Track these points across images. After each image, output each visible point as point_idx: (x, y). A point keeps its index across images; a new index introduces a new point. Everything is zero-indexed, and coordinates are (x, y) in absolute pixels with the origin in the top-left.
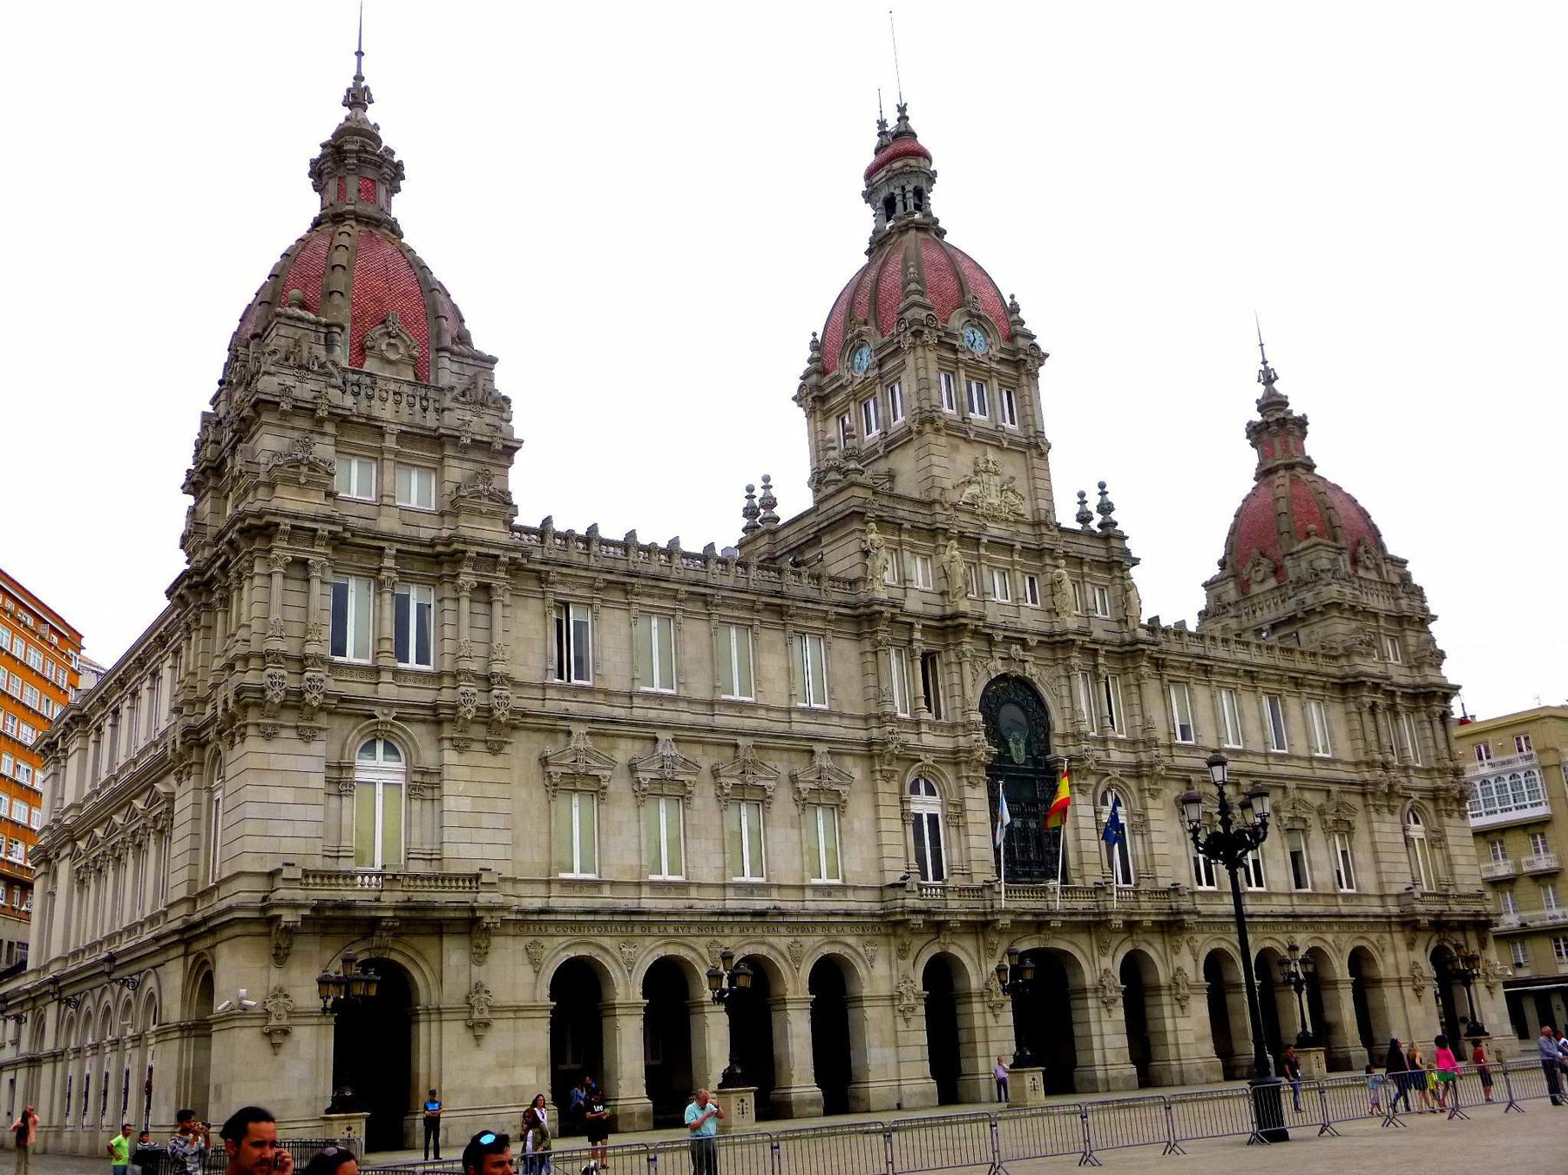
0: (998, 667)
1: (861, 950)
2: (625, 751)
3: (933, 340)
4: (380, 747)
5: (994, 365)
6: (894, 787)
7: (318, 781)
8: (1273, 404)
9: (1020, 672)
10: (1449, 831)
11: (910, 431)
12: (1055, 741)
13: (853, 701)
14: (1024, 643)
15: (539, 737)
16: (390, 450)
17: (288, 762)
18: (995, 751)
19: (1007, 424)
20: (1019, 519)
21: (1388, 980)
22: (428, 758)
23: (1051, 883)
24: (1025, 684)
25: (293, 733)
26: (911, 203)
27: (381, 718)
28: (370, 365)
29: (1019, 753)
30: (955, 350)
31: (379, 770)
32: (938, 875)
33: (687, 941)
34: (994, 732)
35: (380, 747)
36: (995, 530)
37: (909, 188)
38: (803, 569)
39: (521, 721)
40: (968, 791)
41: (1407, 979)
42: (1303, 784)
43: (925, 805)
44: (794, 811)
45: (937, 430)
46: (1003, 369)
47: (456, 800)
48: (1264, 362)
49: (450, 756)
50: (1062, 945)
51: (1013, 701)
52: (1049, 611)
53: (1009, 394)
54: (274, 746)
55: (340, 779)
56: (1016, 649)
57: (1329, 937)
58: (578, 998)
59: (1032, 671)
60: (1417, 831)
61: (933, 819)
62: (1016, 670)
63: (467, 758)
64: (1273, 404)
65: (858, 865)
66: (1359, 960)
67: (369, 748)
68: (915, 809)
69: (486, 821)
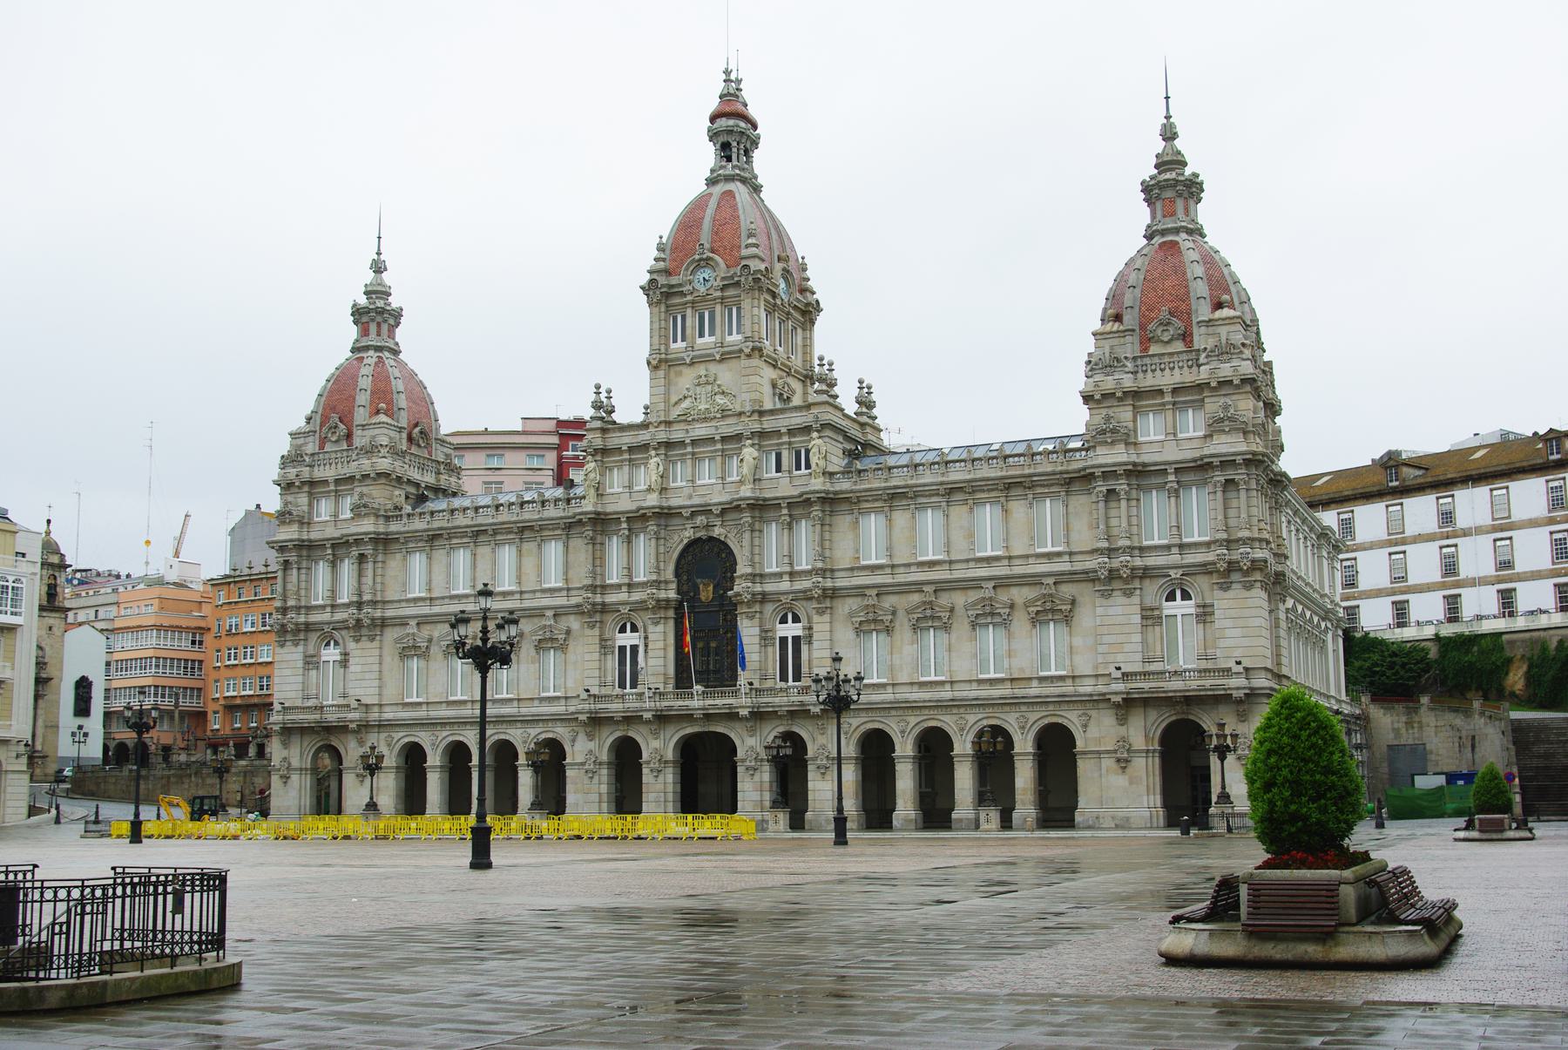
0: (689, 534)
6: (596, 631)
7: (300, 664)
8: (1170, 162)
13: (581, 577)
15: (397, 629)
17: (289, 657)
28: (328, 447)
30: (682, 294)
31: (331, 654)
36: (701, 430)
39: (383, 623)
48: (1168, 117)
50: (720, 729)
51: (705, 558)
54: (286, 650)
55: (311, 662)
56: (700, 520)
59: (717, 532)
61: (634, 648)
62: (701, 534)
63: (360, 645)
64: (1170, 162)
65: (574, 685)
67: (328, 644)
69: (367, 676)
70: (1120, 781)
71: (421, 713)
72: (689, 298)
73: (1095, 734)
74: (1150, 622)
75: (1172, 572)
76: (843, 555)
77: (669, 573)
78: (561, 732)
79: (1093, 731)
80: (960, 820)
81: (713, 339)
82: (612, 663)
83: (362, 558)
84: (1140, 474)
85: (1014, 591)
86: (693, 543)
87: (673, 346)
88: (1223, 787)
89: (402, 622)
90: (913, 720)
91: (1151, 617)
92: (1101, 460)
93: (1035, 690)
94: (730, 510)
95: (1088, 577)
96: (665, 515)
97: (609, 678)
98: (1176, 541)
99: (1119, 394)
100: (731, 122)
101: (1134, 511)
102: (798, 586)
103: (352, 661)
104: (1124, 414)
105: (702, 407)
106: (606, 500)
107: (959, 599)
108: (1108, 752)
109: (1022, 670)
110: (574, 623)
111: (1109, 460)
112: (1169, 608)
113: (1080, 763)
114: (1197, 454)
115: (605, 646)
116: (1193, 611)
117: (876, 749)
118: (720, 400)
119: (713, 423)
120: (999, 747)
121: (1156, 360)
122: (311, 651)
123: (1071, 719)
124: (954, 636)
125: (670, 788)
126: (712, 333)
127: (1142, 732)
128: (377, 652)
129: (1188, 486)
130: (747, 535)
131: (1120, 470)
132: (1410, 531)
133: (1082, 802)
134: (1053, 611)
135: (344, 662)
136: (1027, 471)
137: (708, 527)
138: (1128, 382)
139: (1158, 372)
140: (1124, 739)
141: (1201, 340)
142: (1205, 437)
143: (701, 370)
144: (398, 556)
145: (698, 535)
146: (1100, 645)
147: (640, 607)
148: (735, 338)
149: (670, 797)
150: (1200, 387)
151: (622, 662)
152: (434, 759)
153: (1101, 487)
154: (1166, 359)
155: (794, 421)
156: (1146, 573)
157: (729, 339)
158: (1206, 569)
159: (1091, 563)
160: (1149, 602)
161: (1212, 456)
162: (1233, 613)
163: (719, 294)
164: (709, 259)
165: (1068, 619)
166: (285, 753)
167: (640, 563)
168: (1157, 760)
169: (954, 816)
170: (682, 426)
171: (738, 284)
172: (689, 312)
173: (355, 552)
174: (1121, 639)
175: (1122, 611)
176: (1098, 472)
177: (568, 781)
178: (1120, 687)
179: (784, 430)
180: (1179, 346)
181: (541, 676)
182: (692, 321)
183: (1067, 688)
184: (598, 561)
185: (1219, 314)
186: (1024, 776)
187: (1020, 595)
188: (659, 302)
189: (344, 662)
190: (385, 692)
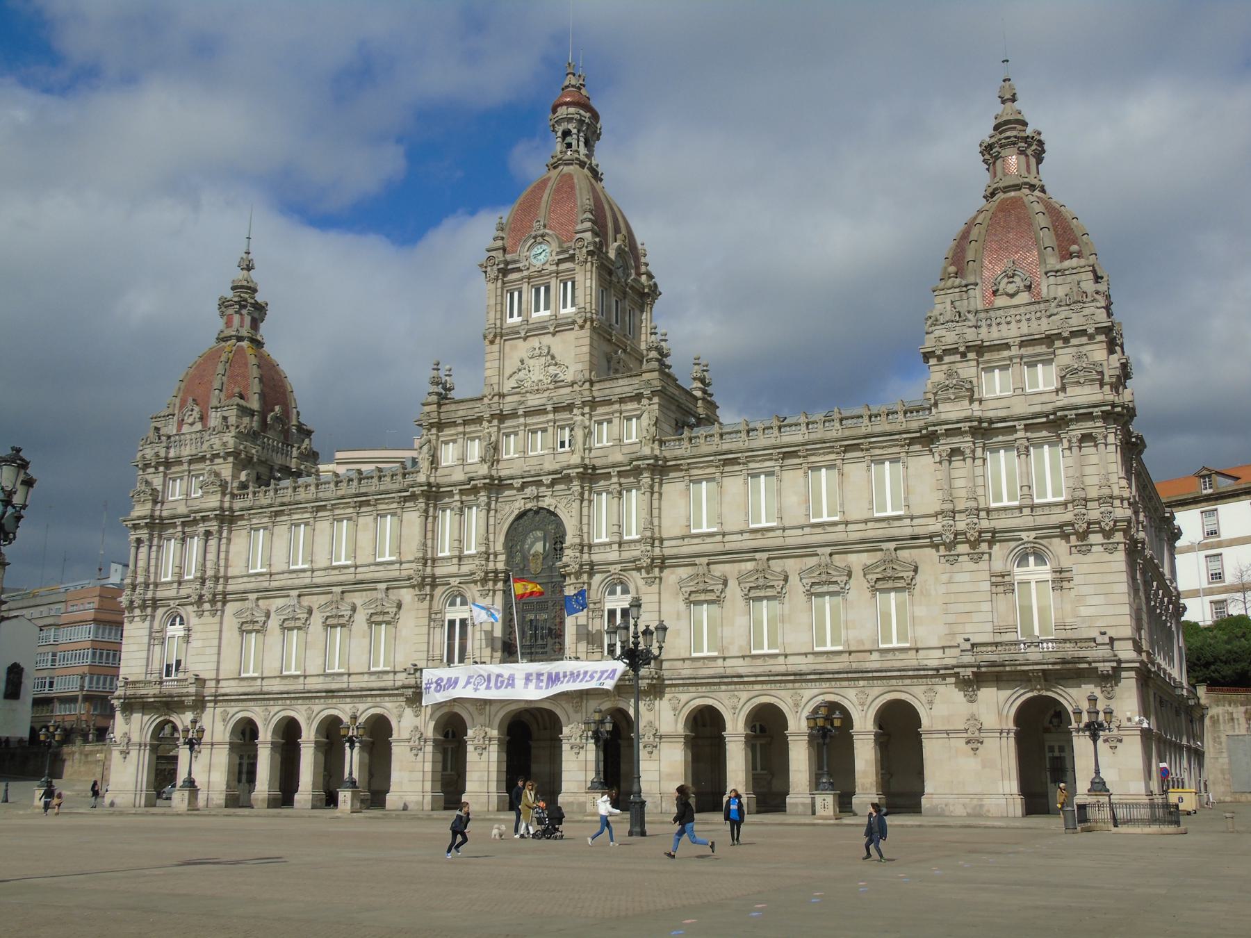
0: (519, 505)
6: (426, 603)
7: (146, 640)
9: (541, 504)
11: (574, 322)
13: (412, 550)
14: (539, 484)
20: (557, 382)
28: (185, 429)
36: (534, 401)
54: (134, 625)
56: (529, 491)
59: (547, 502)
61: (463, 622)
70: (968, 764)
72: (525, 273)
73: (940, 708)
74: (1001, 589)
75: (1024, 535)
76: (671, 525)
77: (499, 547)
78: (389, 708)
79: (940, 709)
80: (796, 804)
81: (548, 313)
82: (440, 636)
83: (208, 534)
84: (985, 431)
85: (852, 558)
86: (521, 516)
87: (509, 321)
88: (1097, 772)
89: (242, 595)
90: (744, 696)
91: (1002, 583)
92: (943, 417)
93: (874, 661)
94: (560, 478)
95: (933, 542)
96: (496, 486)
97: (437, 652)
98: (1027, 502)
99: (962, 349)
100: (572, 110)
101: (979, 471)
102: (626, 555)
103: (194, 636)
104: (968, 370)
105: (535, 378)
106: (440, 472)
107: (792, 566)
108: (957, 731)
109: (862, 642)
110: (407, 595)
111: (953, 416)
112: (1020, 574)
113: (925, 743)
114: (1049, 408)
115: (433, 618)
116: (1049, 577)
117: (705, 730)
118: (552, 370)
119: (546, 394)
120: (837, 723)
121: (1001, 313)
123: (915, 695)
124: (786, 606)
125: (494, 767)
127: (998, 707)
128: (217, 627)
129: (1039, 445)
130: (576, 505)
131: (965, 426)
132: (1225, 535)
133: (929, 788)
134: (892, 578)
135: (187, 638)
136: (863, 431)
137: (537, 497)
138: (971, 335)
139: (1004, 327)
140: (973, 718)
141: (1046, 287)
142: (1057, 392)
143: (534, 342)
144: (244, 532)
145: (529, 506)
146: (944, 612)
147: (469, 579)
148: (570, 310)
149: (494, 776)
150: (1049, 340)
152: (265, 735)
153: (945, 445)
154: (1013, 311)
155: (627, 389)
156: (994, 537)
157: (563, 311)
158: (1063, 531)
159: (935, 526)
160: (998, 566)
161: (1064, 409)
162: (1095, 578)
163: (554, 268)
164: (543, 236)
165: (909, 587)
166: (125, 728)
167: (468, 533)
168: (1012, 742)
169: (788, 800)
170: (516, 398)
171: (572, 258)
172: (525, 287)
173: (201, 529)
174: (969, 607)
175: (971, 577)
176: (940, 429)
177: (394, 758)
178: (968, 658)
180: (1024, 297)
181: (371, 650)
182: (528, 295)
183: (911, 660)
184: (429, 533)
185: (1067, 264)
186: (865, 757)
187: (857, 561)
188: (497, 279)
189: (187, 638)
190: (222, 667)
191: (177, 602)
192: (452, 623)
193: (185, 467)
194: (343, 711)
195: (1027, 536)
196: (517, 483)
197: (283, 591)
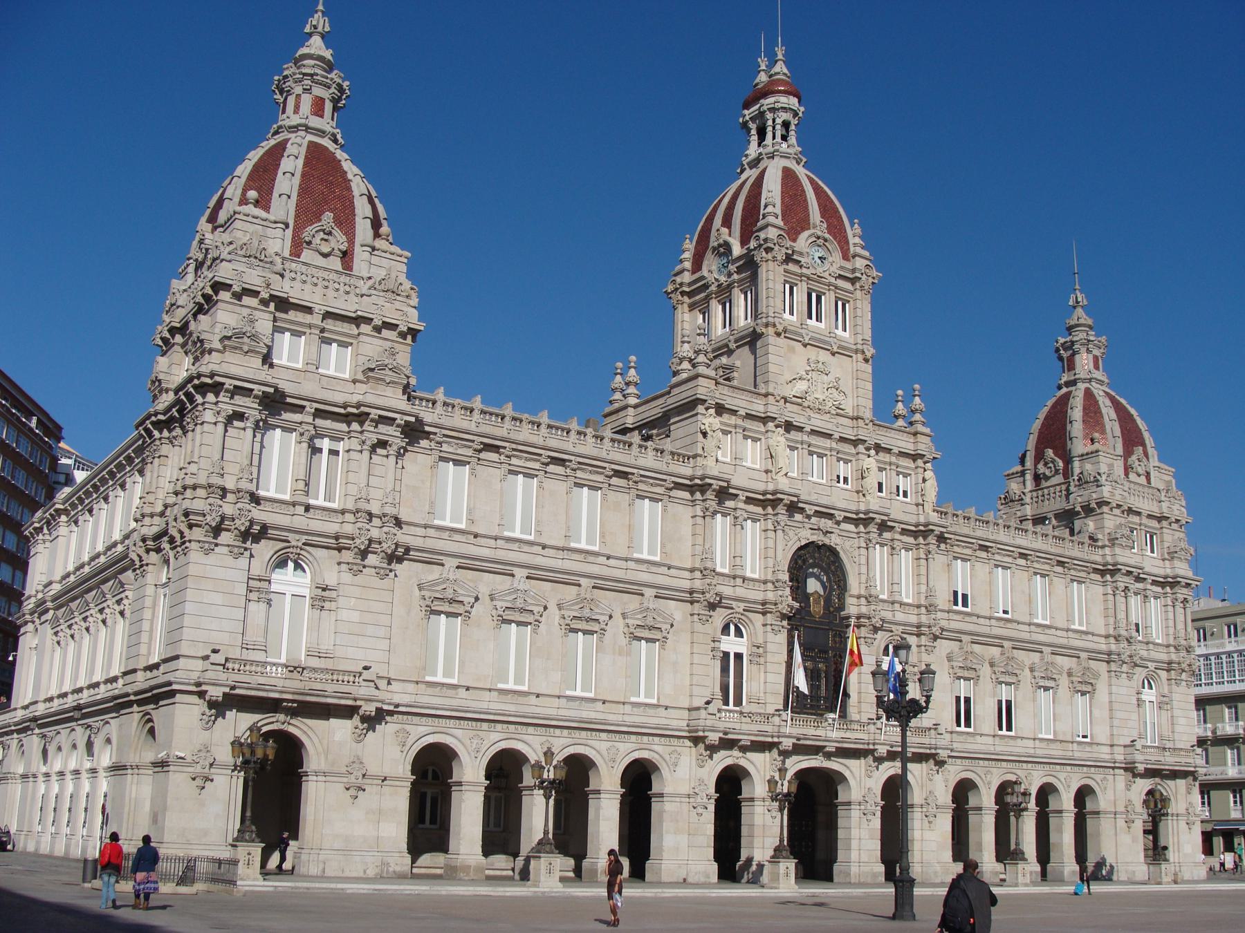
0: (807, 536)
1: (667, 757)
2: (486, 583)
3: (781, 256)
4: (291, 565)
5: (833, 280)
7: (242, 589)
9: (827, 541)
10: (1175, 696)
12: (850, 601)
16: (316, 326)
18: (796, 605)
19: (839, 332)
20: (839, 412)
21: (1106, 813)
22: (331, 579)
23: (832, 715)
24: (833, 552)
25: (225, 550)
26: (778, 134)
27: (294, 543)
29: (817, 609)
32: (738, 702)
33: (525, 737)
34: (798, 588)
35: (291, 565)
36: (818, 422)
37: (779, 121)
38: (649, 443)
40: (770, 636)
41: (1122, 813)
42: (1058, 650)
43: (731, 644)
44: (623, 641)
45: (778, 334)
46: (841, 283)
47: (347, 611)
49: (347, 577)
52: (858, 492)
53: (844, 306)
54: (212, 559)
55: (258, 589)
56: (826, 524)
57: (1062, 776)
58: (432, 773)
59: (833, 540)
60: (1149, 695)
61: (739, 656)
63: (360, 579)
66: (1083, 795)
68: (724, 647)
69: (370, 630)
71: (588, 713)
89: (432, 559)
110: (677, 611)
122: (258, 568)
126: (819, 319)
145: (814, 538)
151: (725, 670)
179: (896, 450)
191: (304, 538)
192: (726, 654)
193: (316, 319)
194: (531, 746)
195: (1151, 665)
196: (810, 510)
197: (504, 569)
